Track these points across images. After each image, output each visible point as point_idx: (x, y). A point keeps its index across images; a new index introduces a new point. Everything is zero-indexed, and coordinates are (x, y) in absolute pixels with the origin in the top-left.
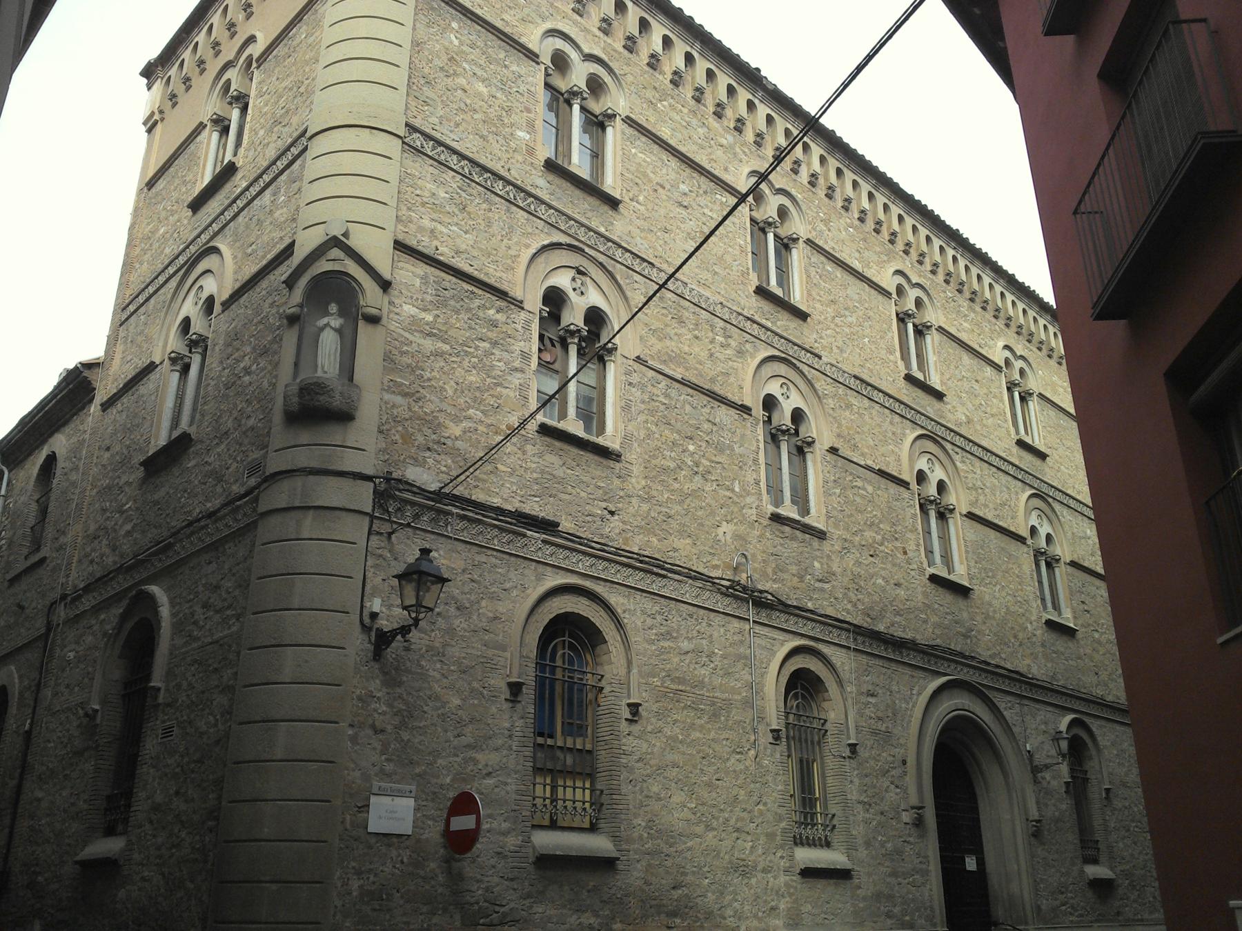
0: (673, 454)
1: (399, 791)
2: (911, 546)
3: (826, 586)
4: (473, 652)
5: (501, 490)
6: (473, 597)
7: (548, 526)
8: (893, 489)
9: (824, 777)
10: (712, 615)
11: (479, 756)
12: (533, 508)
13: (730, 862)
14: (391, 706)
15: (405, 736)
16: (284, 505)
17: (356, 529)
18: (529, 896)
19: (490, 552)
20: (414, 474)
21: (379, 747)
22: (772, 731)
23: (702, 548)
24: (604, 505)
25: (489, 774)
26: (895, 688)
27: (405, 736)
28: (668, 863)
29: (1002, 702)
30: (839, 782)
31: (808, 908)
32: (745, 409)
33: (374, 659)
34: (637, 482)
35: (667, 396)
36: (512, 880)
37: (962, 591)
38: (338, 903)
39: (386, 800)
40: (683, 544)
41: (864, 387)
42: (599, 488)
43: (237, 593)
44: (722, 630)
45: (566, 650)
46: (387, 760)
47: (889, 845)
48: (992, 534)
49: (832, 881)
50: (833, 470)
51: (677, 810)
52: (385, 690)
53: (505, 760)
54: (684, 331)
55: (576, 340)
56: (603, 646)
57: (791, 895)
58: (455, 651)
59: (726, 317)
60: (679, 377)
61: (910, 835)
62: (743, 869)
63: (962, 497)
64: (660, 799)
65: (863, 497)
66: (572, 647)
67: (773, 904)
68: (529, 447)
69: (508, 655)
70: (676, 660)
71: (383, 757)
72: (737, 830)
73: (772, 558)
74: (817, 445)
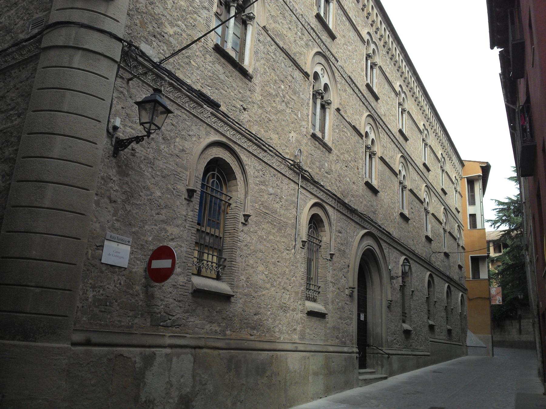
0: (275, 87)
1: (122, 240)
2: (360, 167)
3: (329, 176)
4: (170, 166)
5: (192, 78)
6: (172, 135)
7: (215, 105)
8: (357, 137)
9: (317, 268)
10: (284, 177)
11: (168, 228)
12: (207, 91)
13: (280, 304)
14: (121, 187)
15: (128, 208)
16: (61, 44)
17: (109, 70)
18: (187, 312)
19: (183, 111)
20: (144, 47)
21: (112, 212)
22: (303, 241)
23: (282, 141)
24: (241, 103)
25: (172, 239)
26: (348, 231)
27: (128, 208)
28: (254, 301)
29: (384, 245)
30: (327, 273)
31: (308, 331)
32: (306, 75)
33: (114, 156)
34: (257, 97)
35: (275, 54)
36: (179, 301)
37: (375, 191)
38: (80, 305)
39: (114, 245)
40: (274, 136)
41: (351, 83)
42: (240, 93)
43: (19, 100)
44: (287, 187)
45: (215, 179)
46: (117, 220)
47: (340, 304)
48: (387, 170)
49: (318, 319)
50: (337, 120)
51: (260, 276)
52: (117, 176)
53: (181, 233)
54: (284, 22)
55: (236, 5)
56: (234, 181)
57: (302, 323)
58: (160, 164)
59: (303, 23)
60: (281, 46)
61: (347, 301)
62: (284, 308)
63: (379, 149)
64: (253, 268)
65: (346, 137)
66: (218, 178)
67: (295, 327)
68: (208, 56)
69: (188, 173)
70: (266, 197)
71: (114, 218)
72: (284, 288)
73: (310, 156)
74: (332, 105)
